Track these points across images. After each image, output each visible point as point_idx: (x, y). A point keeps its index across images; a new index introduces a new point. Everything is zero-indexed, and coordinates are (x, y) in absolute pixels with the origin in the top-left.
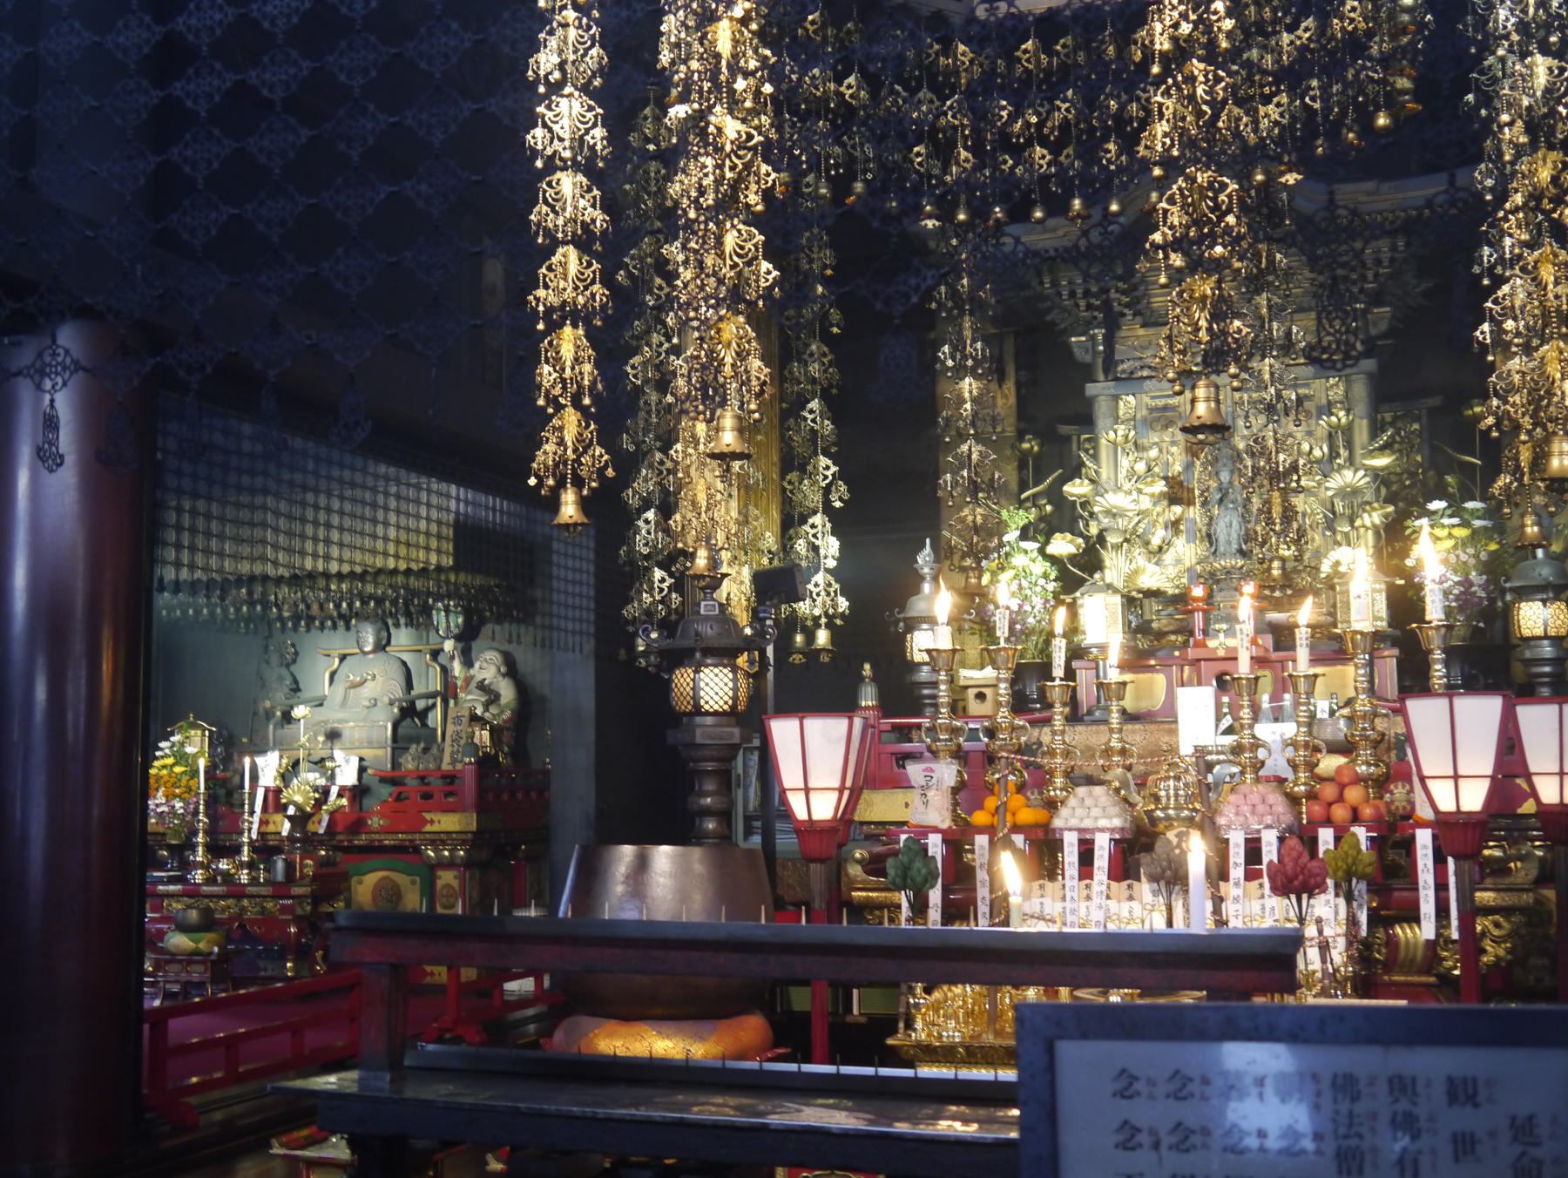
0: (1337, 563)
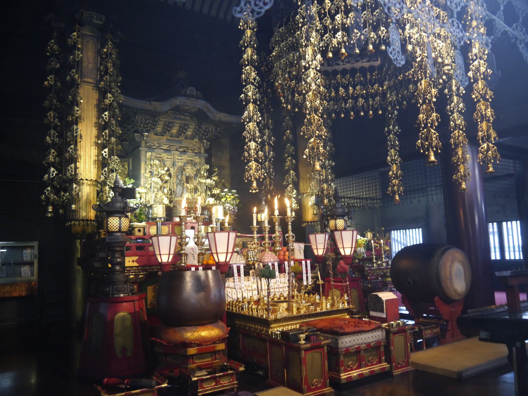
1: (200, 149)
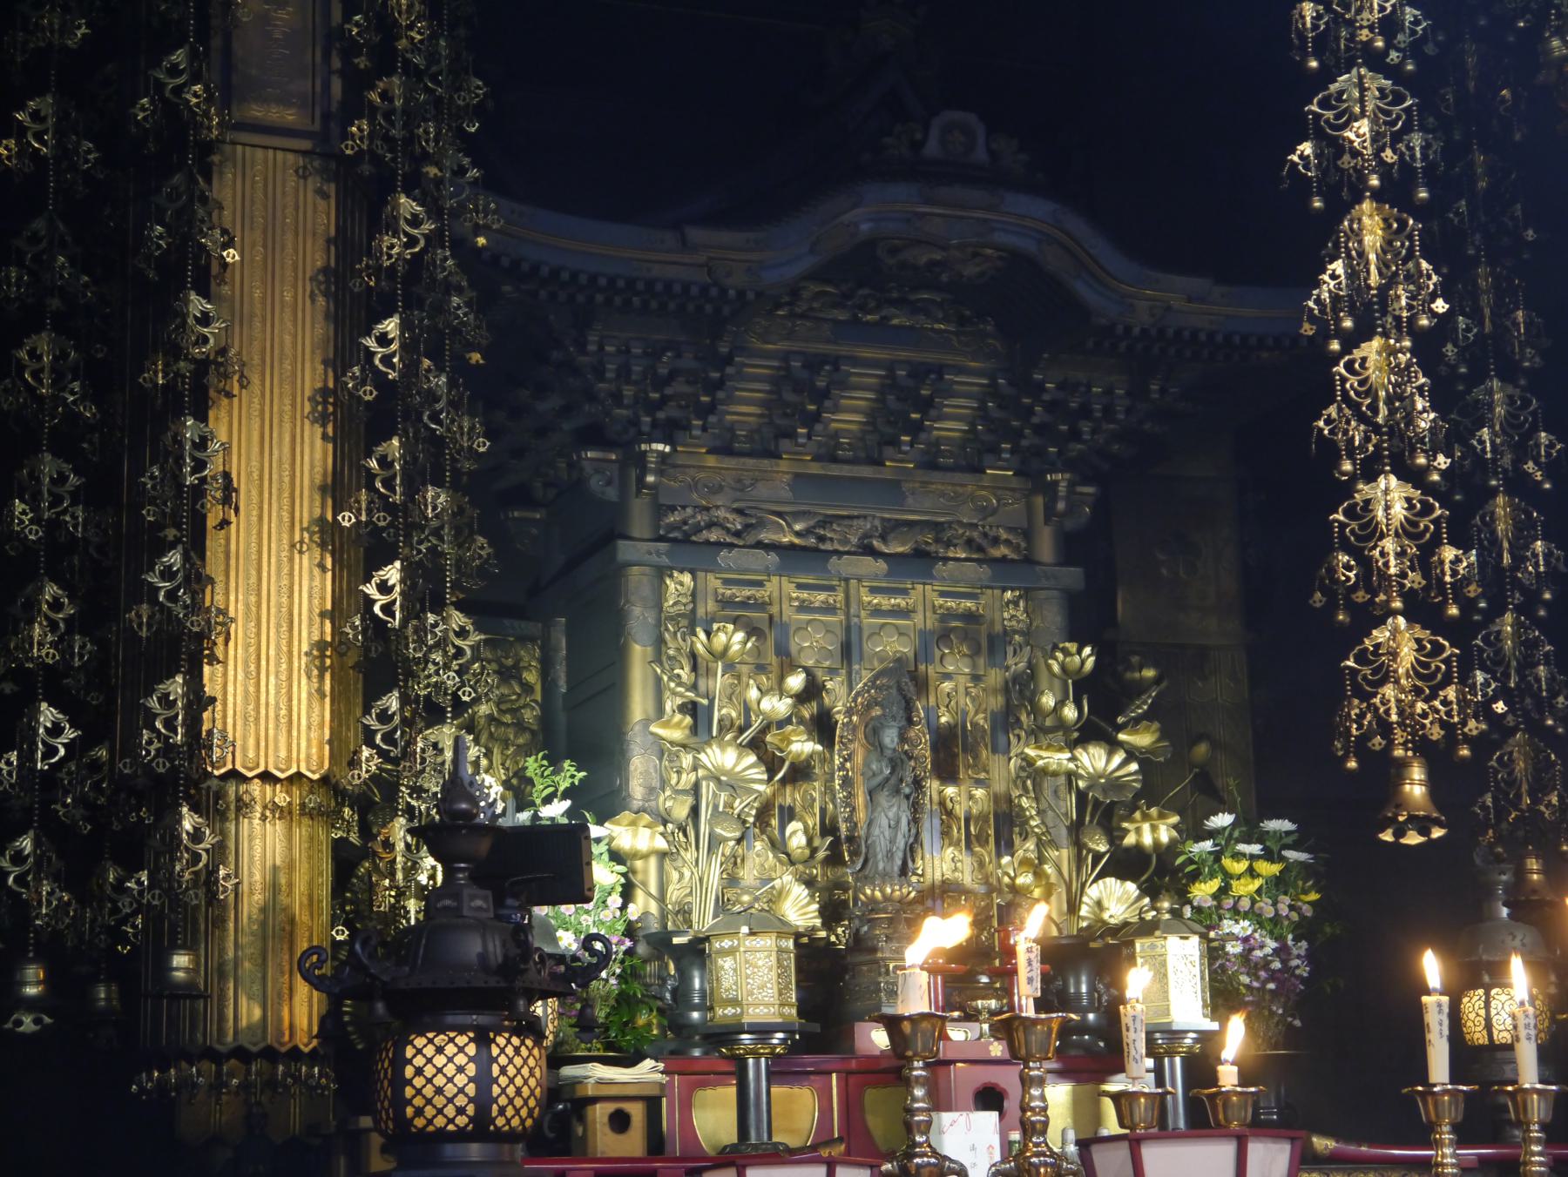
1: (1028, 534)
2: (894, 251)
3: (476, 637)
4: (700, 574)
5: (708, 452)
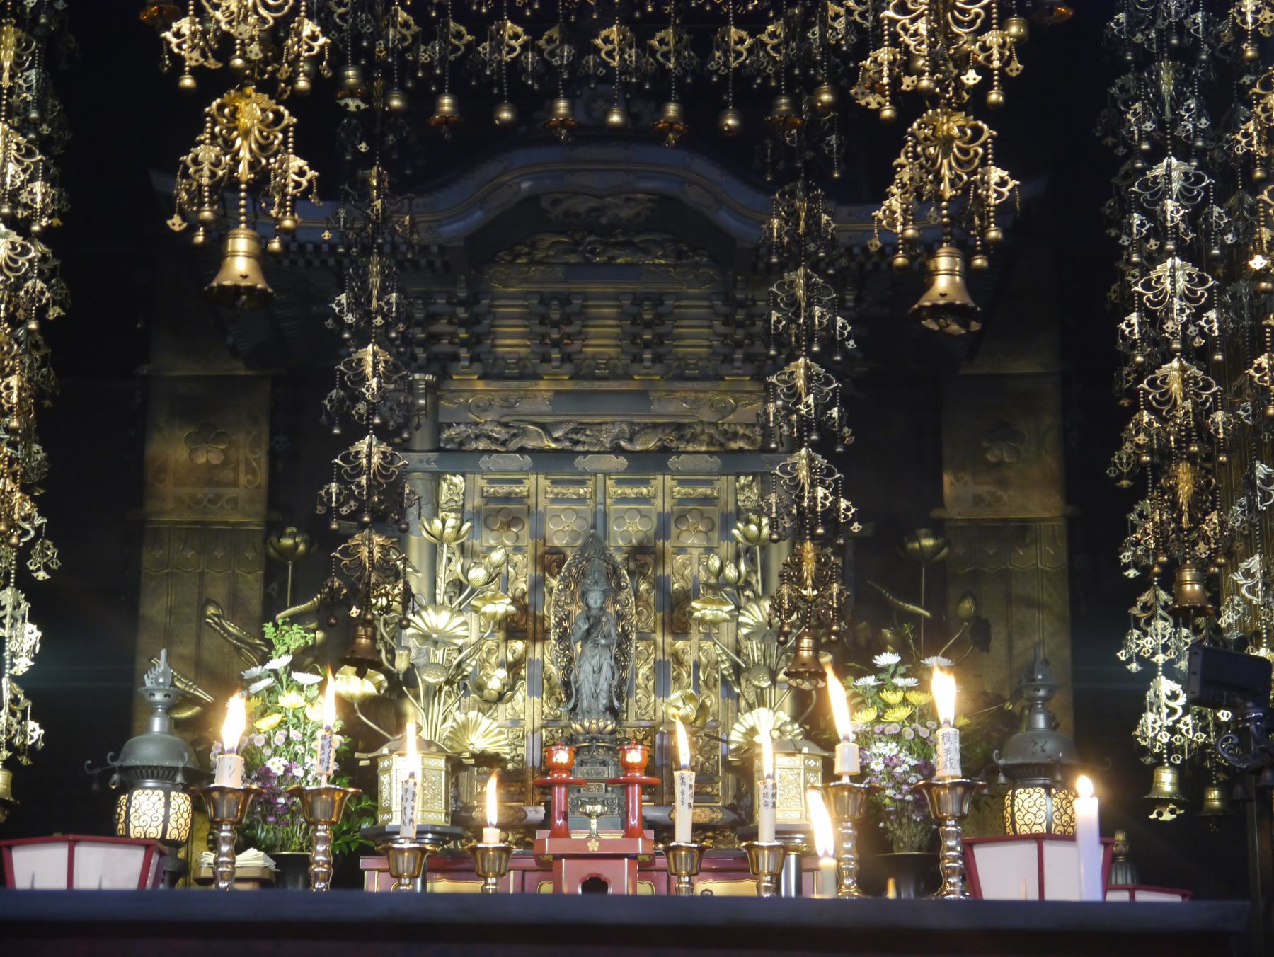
0: (752, 731)
2: (556, 203)
3: (39, 521)
4: (469, 476)
5: (479, 378)
